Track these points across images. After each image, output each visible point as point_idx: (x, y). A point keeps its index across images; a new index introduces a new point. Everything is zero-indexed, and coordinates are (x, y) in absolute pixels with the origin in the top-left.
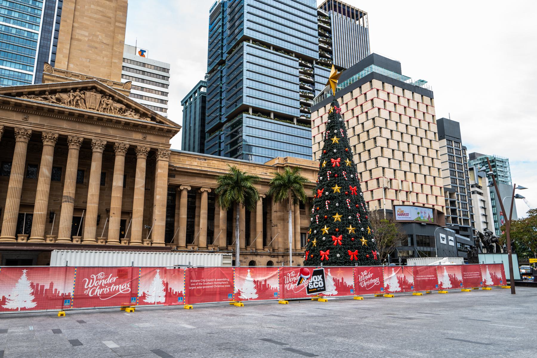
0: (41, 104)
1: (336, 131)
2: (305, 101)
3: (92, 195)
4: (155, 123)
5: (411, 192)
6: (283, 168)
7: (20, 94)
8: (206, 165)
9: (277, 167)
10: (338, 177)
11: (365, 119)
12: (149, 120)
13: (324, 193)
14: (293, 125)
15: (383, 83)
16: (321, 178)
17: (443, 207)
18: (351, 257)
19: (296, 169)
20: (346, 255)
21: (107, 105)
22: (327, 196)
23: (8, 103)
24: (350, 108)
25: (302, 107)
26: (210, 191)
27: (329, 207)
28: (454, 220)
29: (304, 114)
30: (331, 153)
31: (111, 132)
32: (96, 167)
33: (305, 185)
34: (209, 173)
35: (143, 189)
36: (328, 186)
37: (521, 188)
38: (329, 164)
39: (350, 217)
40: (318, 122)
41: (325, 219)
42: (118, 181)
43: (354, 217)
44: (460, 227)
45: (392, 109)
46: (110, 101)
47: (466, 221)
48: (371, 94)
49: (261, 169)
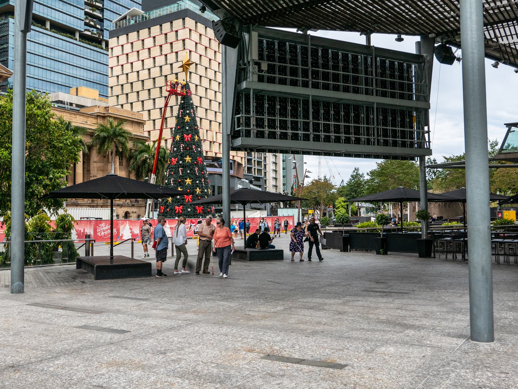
1: (188, 111)
2: (91, 12)
5: (214, 142)
6: (104, 117)
9: (98, 116)
10: (189, 149)
13: (178, 162)
14: (75, 42)
15: (196, 23)
16: (175, 149)
17: (242, 158)
18: (198, 211)
19: (122, 121)
20: (195, 209)
22: (181, 164)
25: (86, 18)
27: (182, 173)
28: (249, 169)
29: (88, 28)
30: (184, 130)
33: (130, 137)
36: (181, 156)
37: (309, 172)
38: (182, 139)
39: (198, 182)
40: (117, 51)
41: (180, 182)
43: (200, 181)
44: (254, 177)
45: (203, 53)
47: (259, 171)
48: (183, 34)
49: (81, 118)
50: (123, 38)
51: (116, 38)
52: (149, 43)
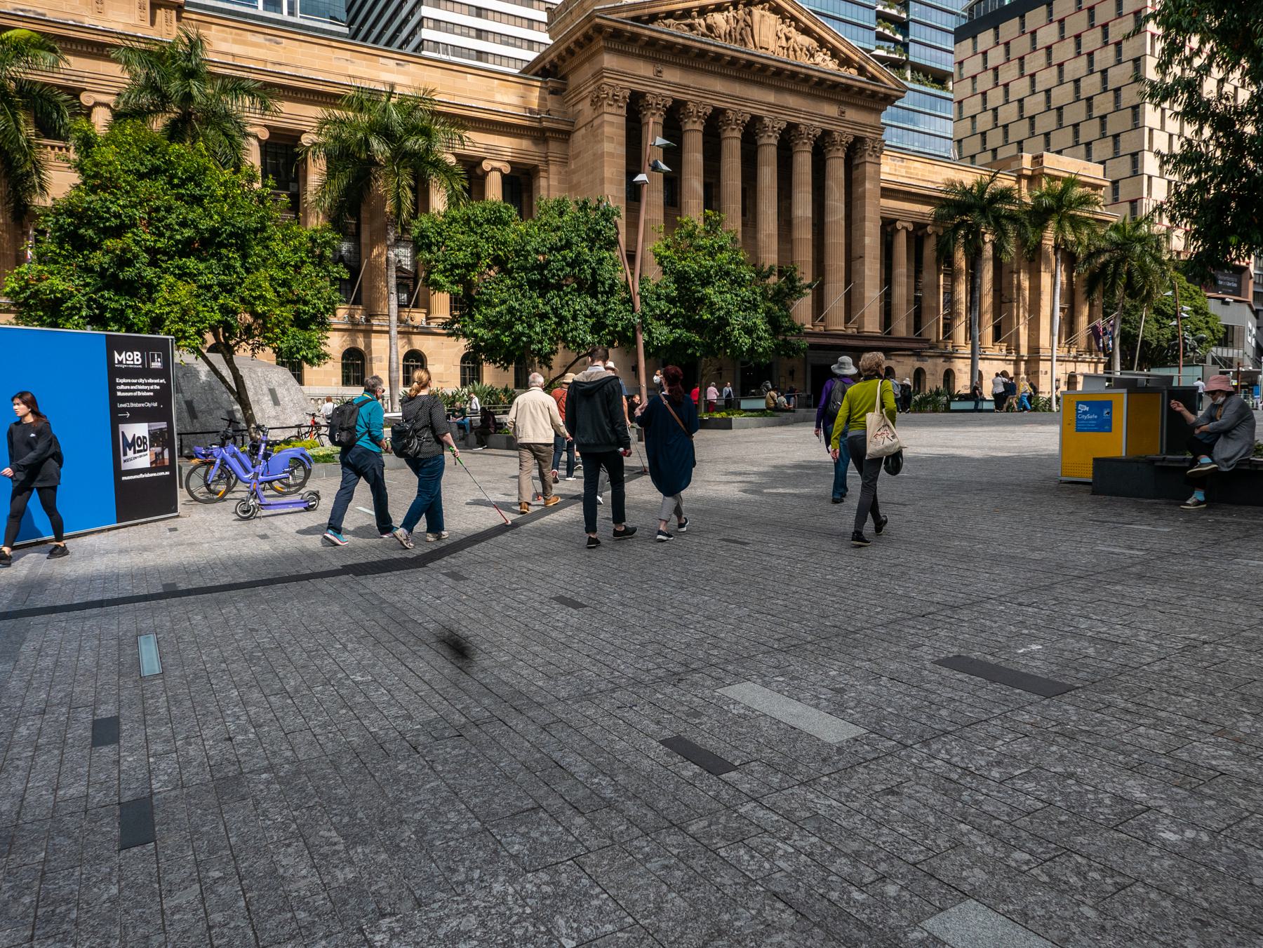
0: (689, 39)
3: (769, 236)
4: (864, 79)
7: (653, 18)
8: (903, 172)
11: (1112, 61)
12: (853, 72)
21: (788, 39)
23: (635, 38)
24: (1070, 31)
26: (911, 229)
31: (791, 101)
32: (768, 176)
34: (913, 190)
35: (843, 223)
42: (803, 207)
46: (793, 33)
50: (986, 38)
51: (970, 41)
52: (1048, 35)
